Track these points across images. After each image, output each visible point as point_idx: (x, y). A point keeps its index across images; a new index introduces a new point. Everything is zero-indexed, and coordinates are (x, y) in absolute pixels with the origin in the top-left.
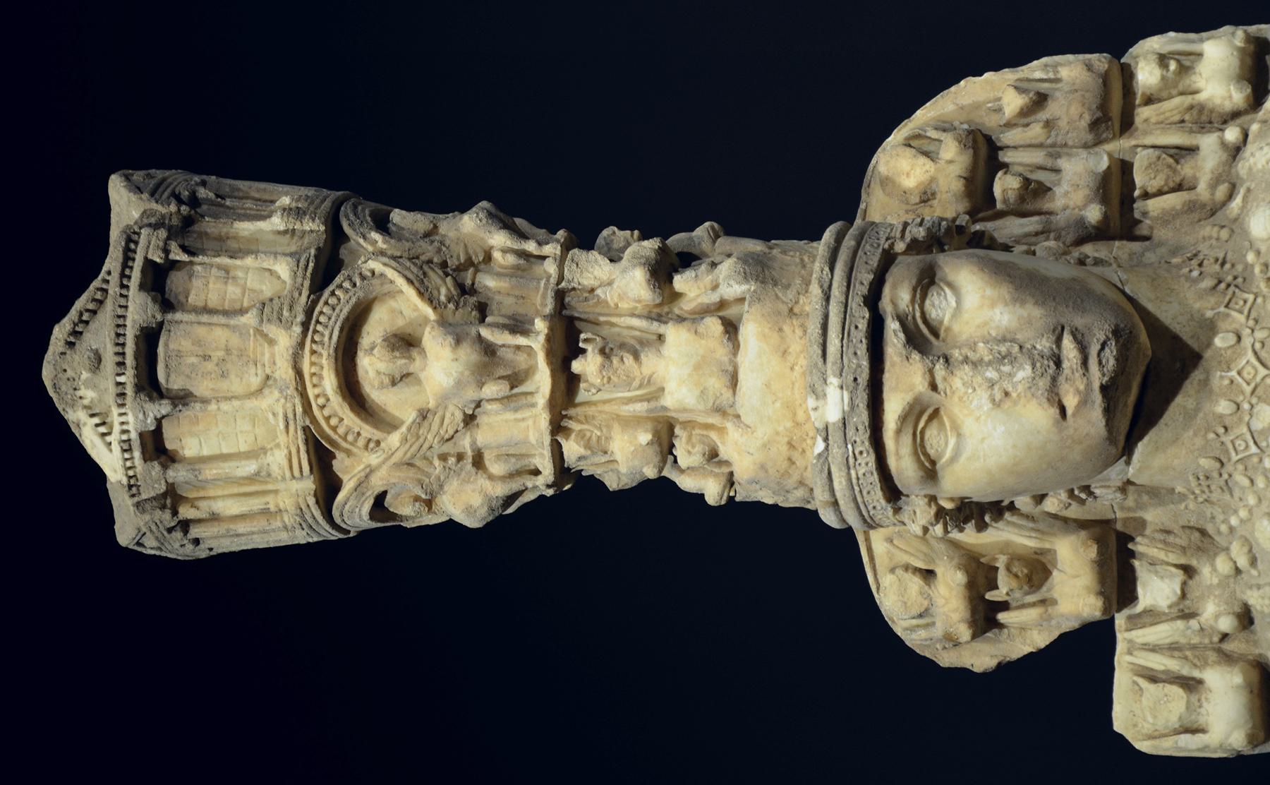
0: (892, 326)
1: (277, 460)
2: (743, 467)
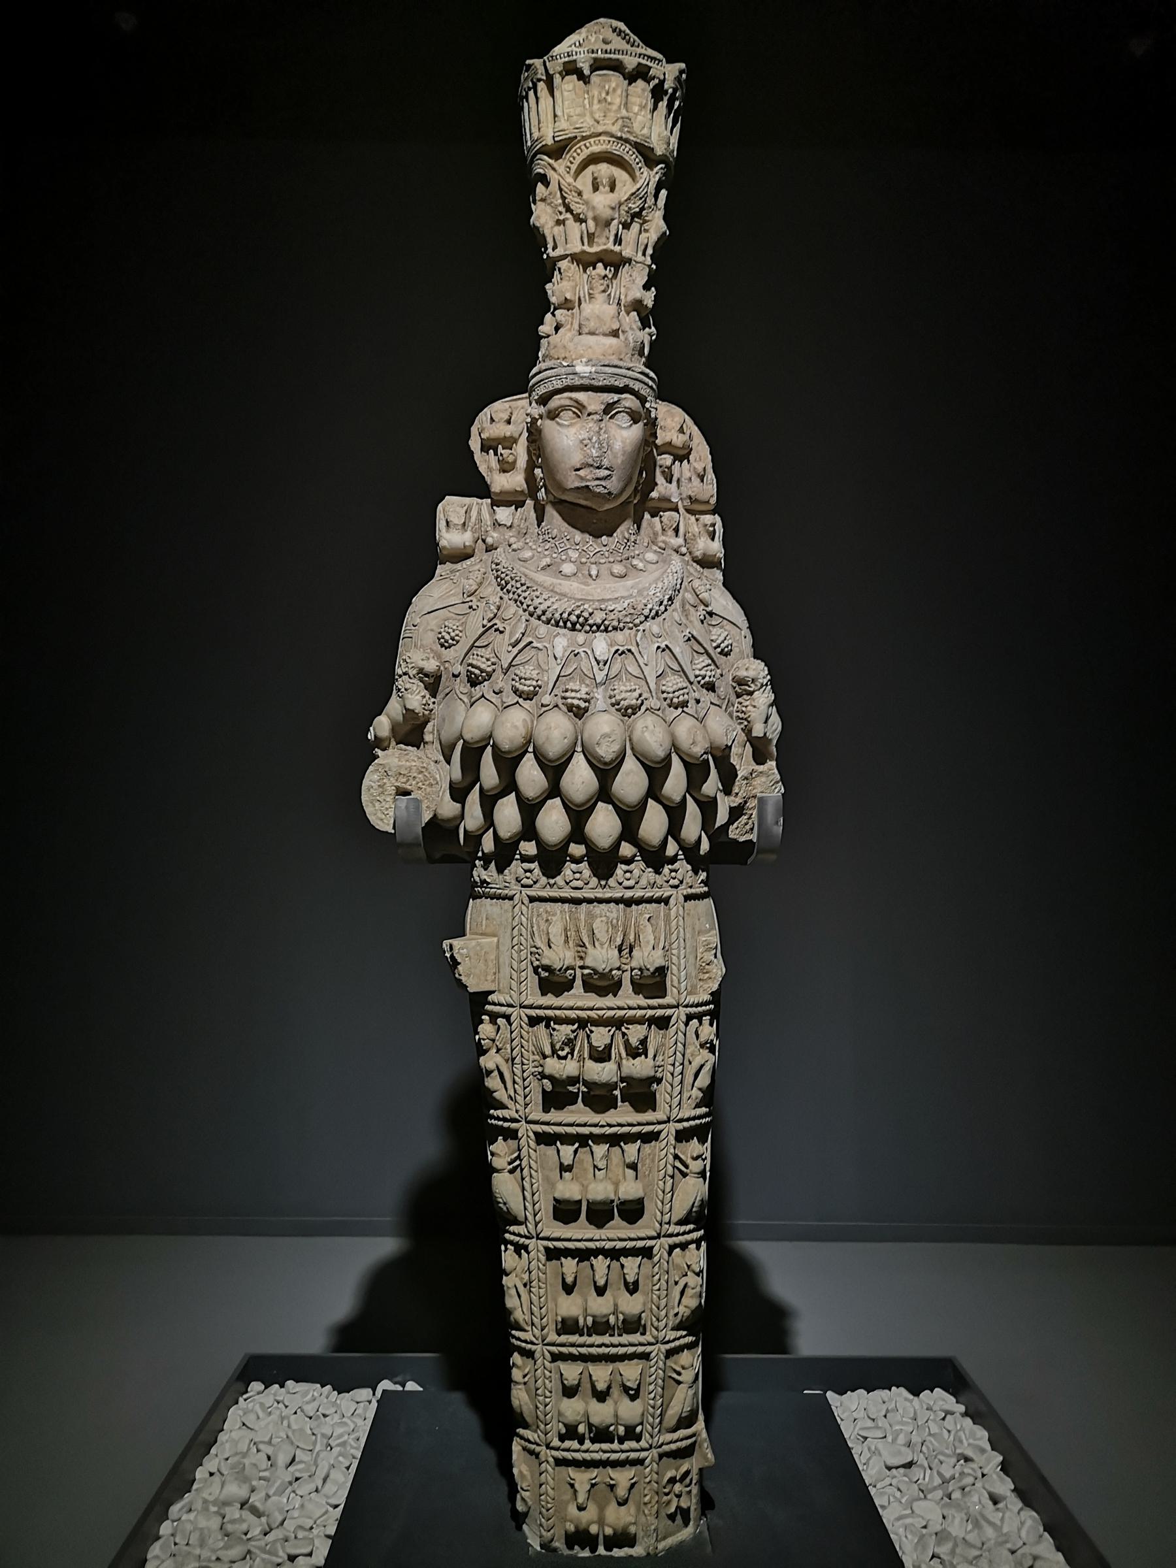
0: (616, 397)
1: (563, 124)
2: (554, 339)
